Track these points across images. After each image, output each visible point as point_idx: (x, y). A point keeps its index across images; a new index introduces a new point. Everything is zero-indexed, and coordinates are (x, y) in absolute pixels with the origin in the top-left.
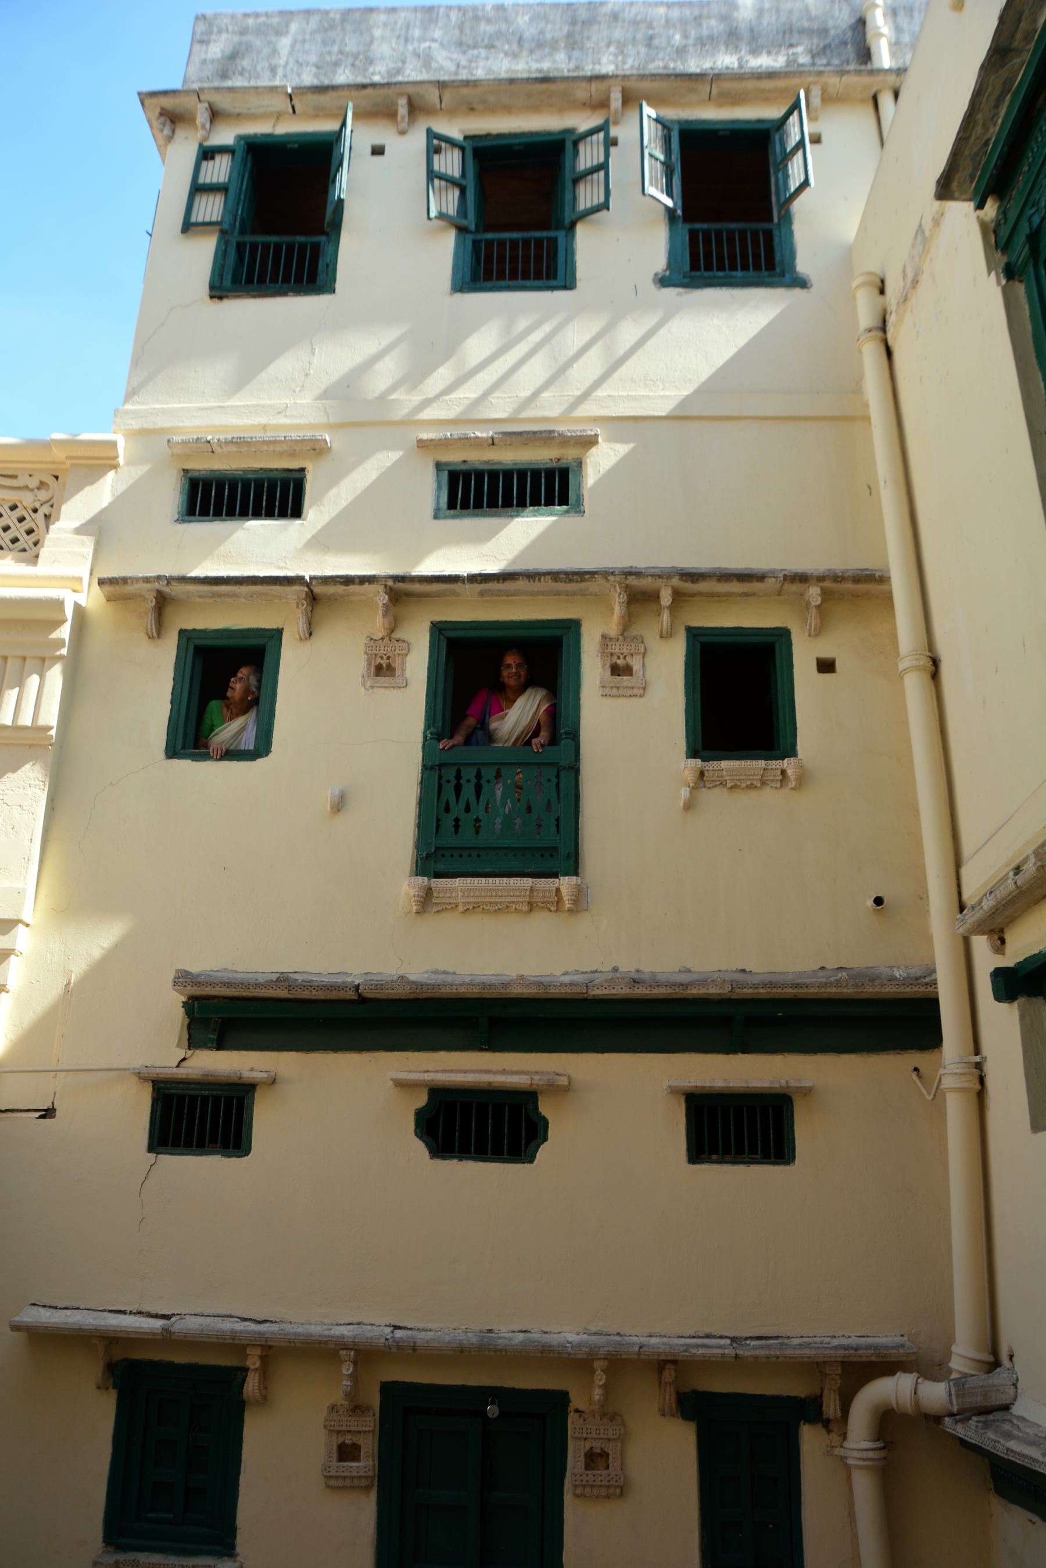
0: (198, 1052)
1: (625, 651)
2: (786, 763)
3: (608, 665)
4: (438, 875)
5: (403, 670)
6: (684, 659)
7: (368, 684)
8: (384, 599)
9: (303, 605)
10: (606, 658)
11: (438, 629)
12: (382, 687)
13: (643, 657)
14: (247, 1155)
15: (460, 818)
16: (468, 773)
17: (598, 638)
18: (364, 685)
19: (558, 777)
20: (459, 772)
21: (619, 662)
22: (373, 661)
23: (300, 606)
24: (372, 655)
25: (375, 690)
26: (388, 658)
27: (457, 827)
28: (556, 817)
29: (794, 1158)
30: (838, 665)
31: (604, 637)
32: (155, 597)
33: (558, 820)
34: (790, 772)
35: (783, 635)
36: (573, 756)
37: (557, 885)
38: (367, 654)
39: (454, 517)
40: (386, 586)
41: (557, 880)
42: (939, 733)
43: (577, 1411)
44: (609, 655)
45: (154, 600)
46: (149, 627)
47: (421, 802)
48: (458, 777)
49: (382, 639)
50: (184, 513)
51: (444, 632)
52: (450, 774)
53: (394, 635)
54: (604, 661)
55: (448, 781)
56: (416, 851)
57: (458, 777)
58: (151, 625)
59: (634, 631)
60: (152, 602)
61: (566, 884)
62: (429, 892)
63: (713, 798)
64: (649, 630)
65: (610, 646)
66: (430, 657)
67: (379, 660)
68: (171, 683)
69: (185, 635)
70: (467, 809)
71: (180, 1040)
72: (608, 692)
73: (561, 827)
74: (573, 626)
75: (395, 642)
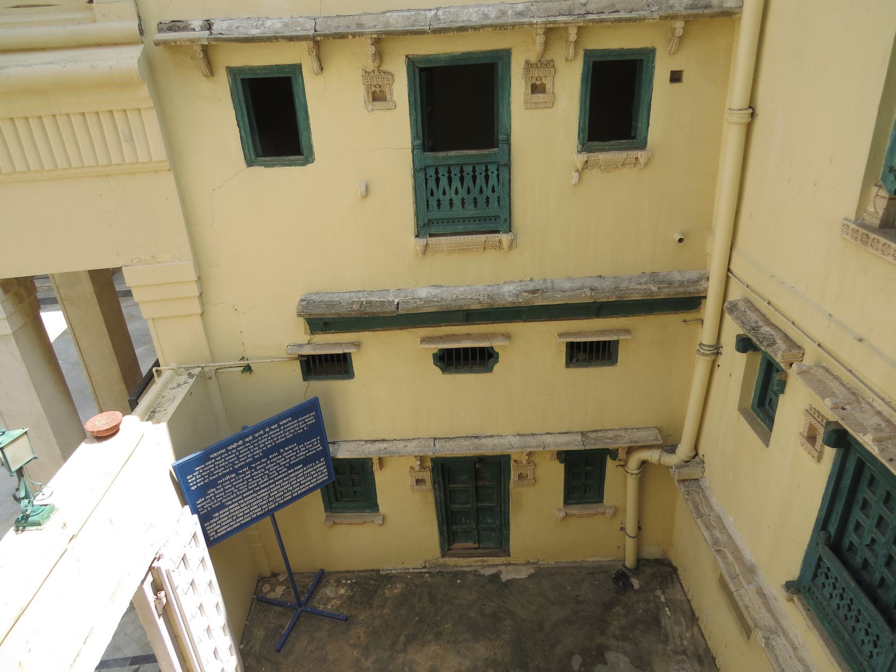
0: (316, 335)
1: (541, 75)
2: (639, 154)
3: (530, 85)
4: (431, 235)
5: (392, 95)
6: (581, 76)
7: (369, 108)
8: (372, 50)
9: (313, 52)
10: (528, 81)
11: (411, 62)
12: (380, 110)
13: (553, 77)
14: (353, 378)
15: (440, 199)
16: (442, 171)
17: (523, 64)
18: (366, 108)
19: (498, 170)
21: (537, 83)
22: (370, 90)
23: (311, 53)
24: (368, 85)
25: (375, 111)
26: (380, 87)
27: (439, 205)
28: (498, 196)
29: (617, 362)
30: (685, 77)
31: (527, 62)
32: (201, 50)
33: (498, 198)
34: (642, 160)
35: (649, 54)
36: (508, 152)
37: (500, 238)
38: (365, 85)
40: (371, 38)
41: (499, 235)
42: (742, 158)
43: (515, 461)
44: (530, 78)
45: (201, 53)
46: (204, 70)
47: (415, 189)
48: (437, 173)
49: (374, 71)
51: (417, 64)
52: (431, 172)
53: (381, 68)
54: (527, 82)
56: (416, 218)
57: (437, 173)
58: (205, 70)
59: (548, 57)
60: (200, 54)
61: (505, 238)
62: (427, 245)
63: (593, 175)
64: (558, 54)
65: (531, 72)
66: (409, 85)
67: (374, 89)
68: (233, 112)
69: (233, 72)
70: (444, 193)
71: (305, 330)
72: (529, 105)
73: (501, 204)
74: (505, 55)
75: (383, 74)
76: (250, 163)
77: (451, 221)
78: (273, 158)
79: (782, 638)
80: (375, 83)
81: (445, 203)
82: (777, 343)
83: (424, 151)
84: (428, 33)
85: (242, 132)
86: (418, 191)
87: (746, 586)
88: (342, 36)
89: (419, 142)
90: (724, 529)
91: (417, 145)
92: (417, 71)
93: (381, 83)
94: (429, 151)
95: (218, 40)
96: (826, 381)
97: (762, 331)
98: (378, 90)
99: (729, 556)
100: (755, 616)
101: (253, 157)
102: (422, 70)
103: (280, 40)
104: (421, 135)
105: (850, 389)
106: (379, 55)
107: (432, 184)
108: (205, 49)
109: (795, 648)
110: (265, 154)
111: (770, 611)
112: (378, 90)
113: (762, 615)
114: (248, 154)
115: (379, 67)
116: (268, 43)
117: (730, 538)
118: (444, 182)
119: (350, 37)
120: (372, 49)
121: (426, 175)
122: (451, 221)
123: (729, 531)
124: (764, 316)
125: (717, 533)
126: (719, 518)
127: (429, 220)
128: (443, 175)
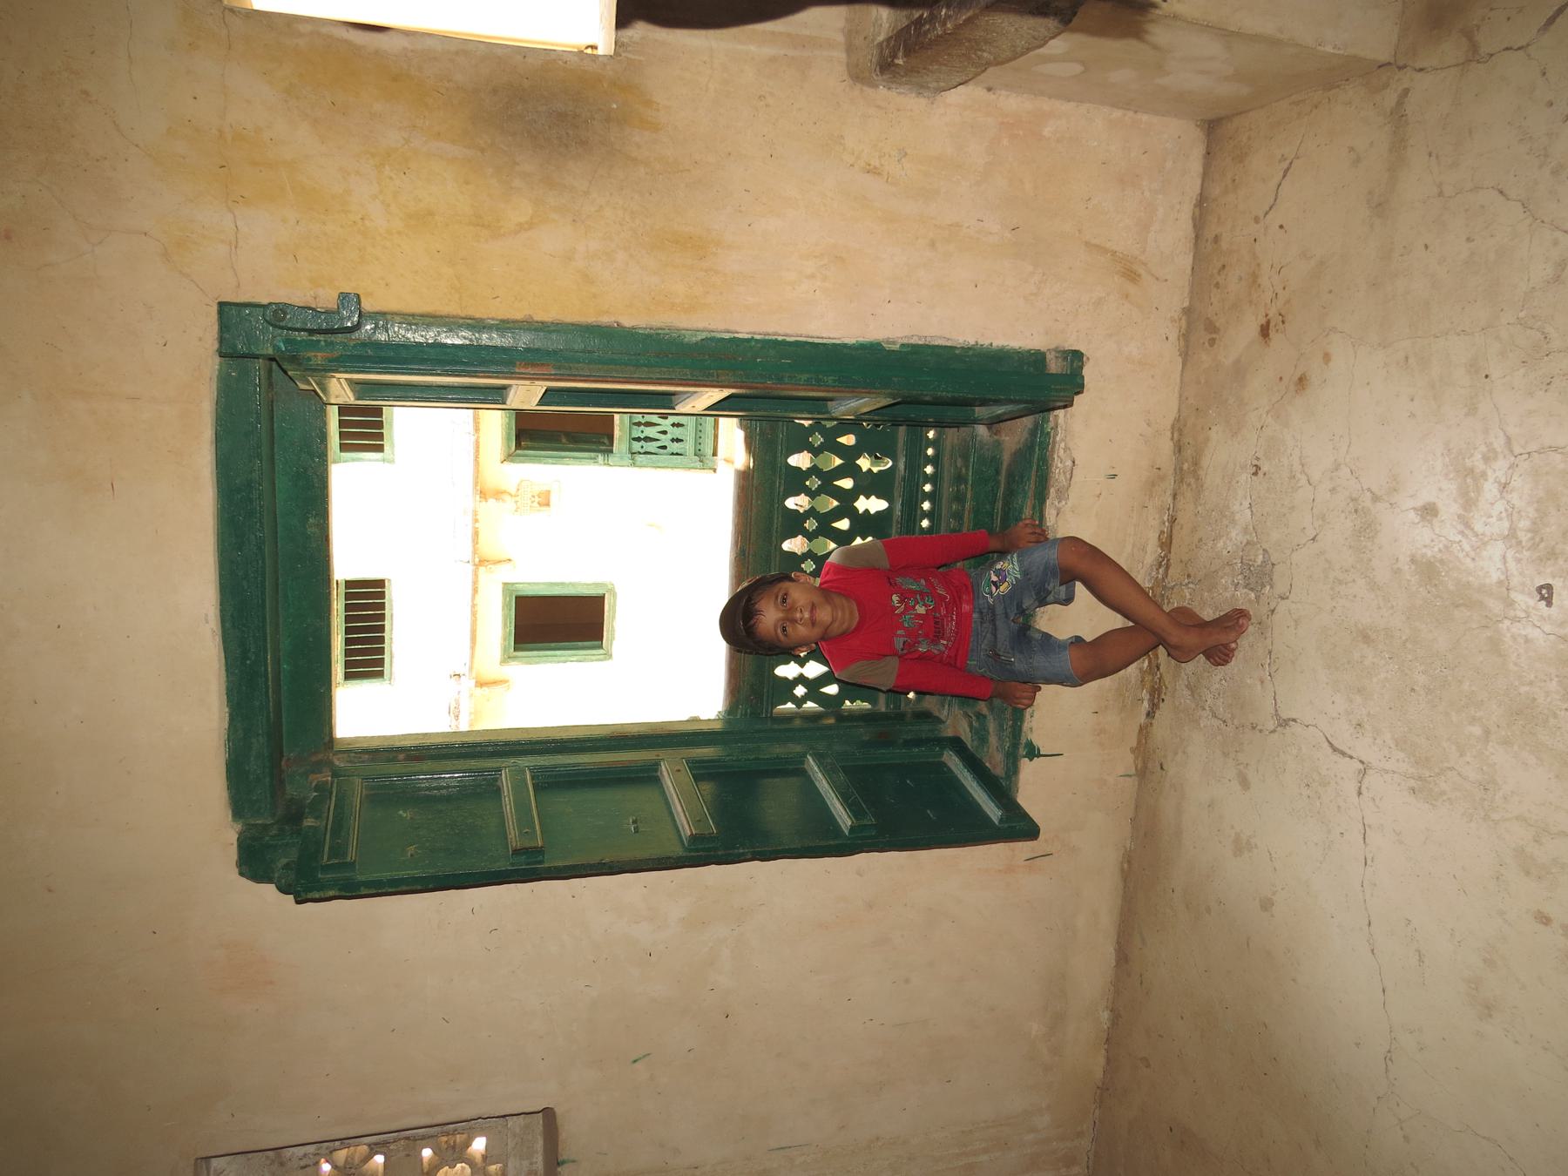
4: (715, 454)
16: (637, 433)
20: (634, 439)
26: (534, 497)
27: (678, 440)
39: (392, 446)
48: (638, 439)
49: (516, 502)
50: (381, 679)
51: (511, 452)
52: (637, 446)
53: (513, 492)
55: (642, 447)
57: (638, 439)
67: (535, 504)
69: (507, 658)
70: (664, 432)
76: (608, 656)
77: (700, 428)
78: (605, 629)
80: (529, 502)
81: (677, 432)
83: (611, 451)
84: (478, 437)
85: (572, 659)
86: (660, 465)
88: (476, 534)
89: (600, 457)
91: (604, 460)
92: (519, 452)
93: (530, 496)
94: (612, 445)
95: (471, 668)
98: (537, 499)
101: (601, 651)
102: (518, 446)
103: (475, 602)
104: (593, 454)
106: (498, 494)
107: (651, 447)
108: (481, 684)
110: (600, 638)
112: (537, 499)
114: (598, 657)
115: (511, 495)
116: (477, 616)
118: (651, 432)
119: (477, 525)
120: (492, 501)
121: (640, 453)
122: (700, 428)
127: (695, 455)
128: (642, 432)
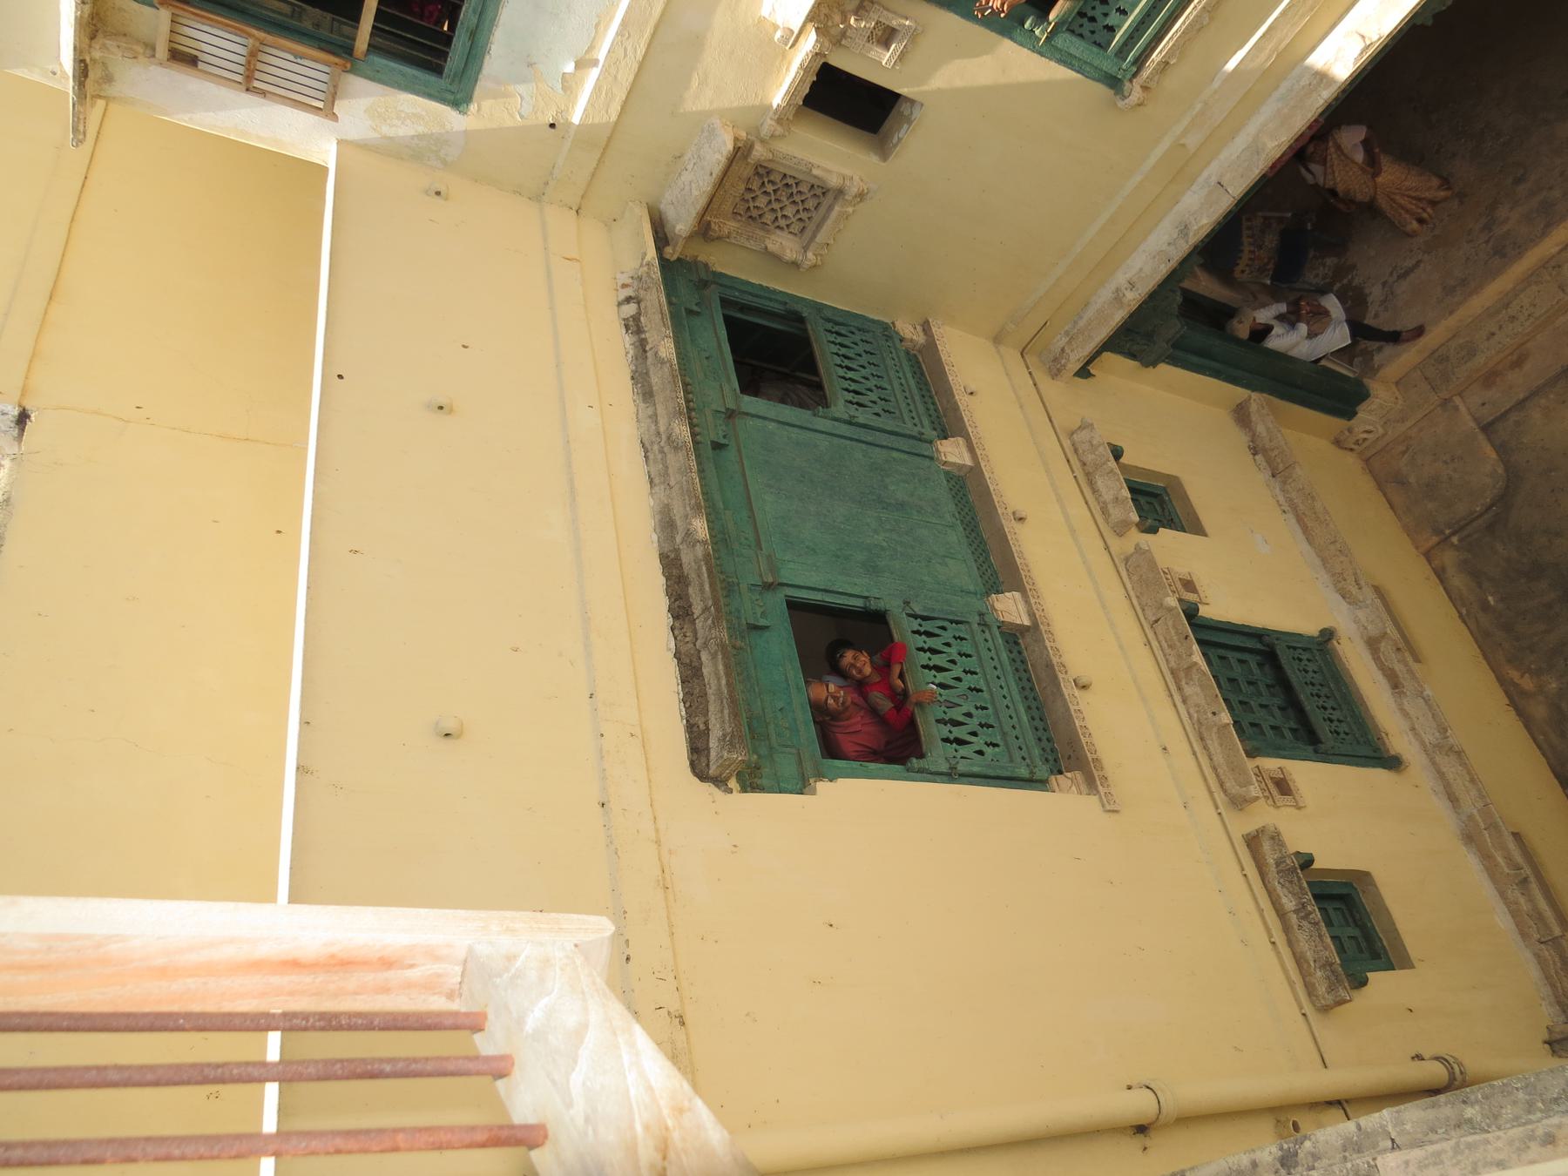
79: (1427, 741)
82: (1275, 860)
87: (1475, 812)
90: (1515, 913)
96: (1225, 768)
97: (1294, 903)
99: (1500, 860)
100: (1461, 768)
105: (1205, 748)
109: (1413, 729)
111: (1441, 775)
113: (1453, 770)
117: (1502, 894)
123: (1506, 909)
124: (1290, 943)
125: (1525, 906)
126: (1524, 935)
